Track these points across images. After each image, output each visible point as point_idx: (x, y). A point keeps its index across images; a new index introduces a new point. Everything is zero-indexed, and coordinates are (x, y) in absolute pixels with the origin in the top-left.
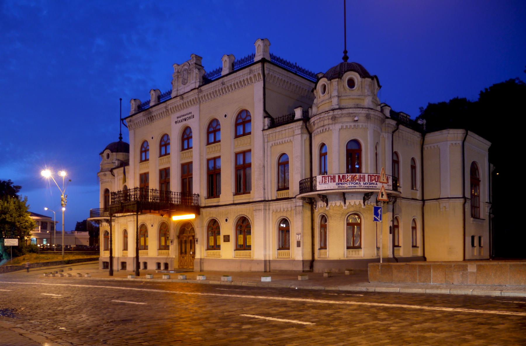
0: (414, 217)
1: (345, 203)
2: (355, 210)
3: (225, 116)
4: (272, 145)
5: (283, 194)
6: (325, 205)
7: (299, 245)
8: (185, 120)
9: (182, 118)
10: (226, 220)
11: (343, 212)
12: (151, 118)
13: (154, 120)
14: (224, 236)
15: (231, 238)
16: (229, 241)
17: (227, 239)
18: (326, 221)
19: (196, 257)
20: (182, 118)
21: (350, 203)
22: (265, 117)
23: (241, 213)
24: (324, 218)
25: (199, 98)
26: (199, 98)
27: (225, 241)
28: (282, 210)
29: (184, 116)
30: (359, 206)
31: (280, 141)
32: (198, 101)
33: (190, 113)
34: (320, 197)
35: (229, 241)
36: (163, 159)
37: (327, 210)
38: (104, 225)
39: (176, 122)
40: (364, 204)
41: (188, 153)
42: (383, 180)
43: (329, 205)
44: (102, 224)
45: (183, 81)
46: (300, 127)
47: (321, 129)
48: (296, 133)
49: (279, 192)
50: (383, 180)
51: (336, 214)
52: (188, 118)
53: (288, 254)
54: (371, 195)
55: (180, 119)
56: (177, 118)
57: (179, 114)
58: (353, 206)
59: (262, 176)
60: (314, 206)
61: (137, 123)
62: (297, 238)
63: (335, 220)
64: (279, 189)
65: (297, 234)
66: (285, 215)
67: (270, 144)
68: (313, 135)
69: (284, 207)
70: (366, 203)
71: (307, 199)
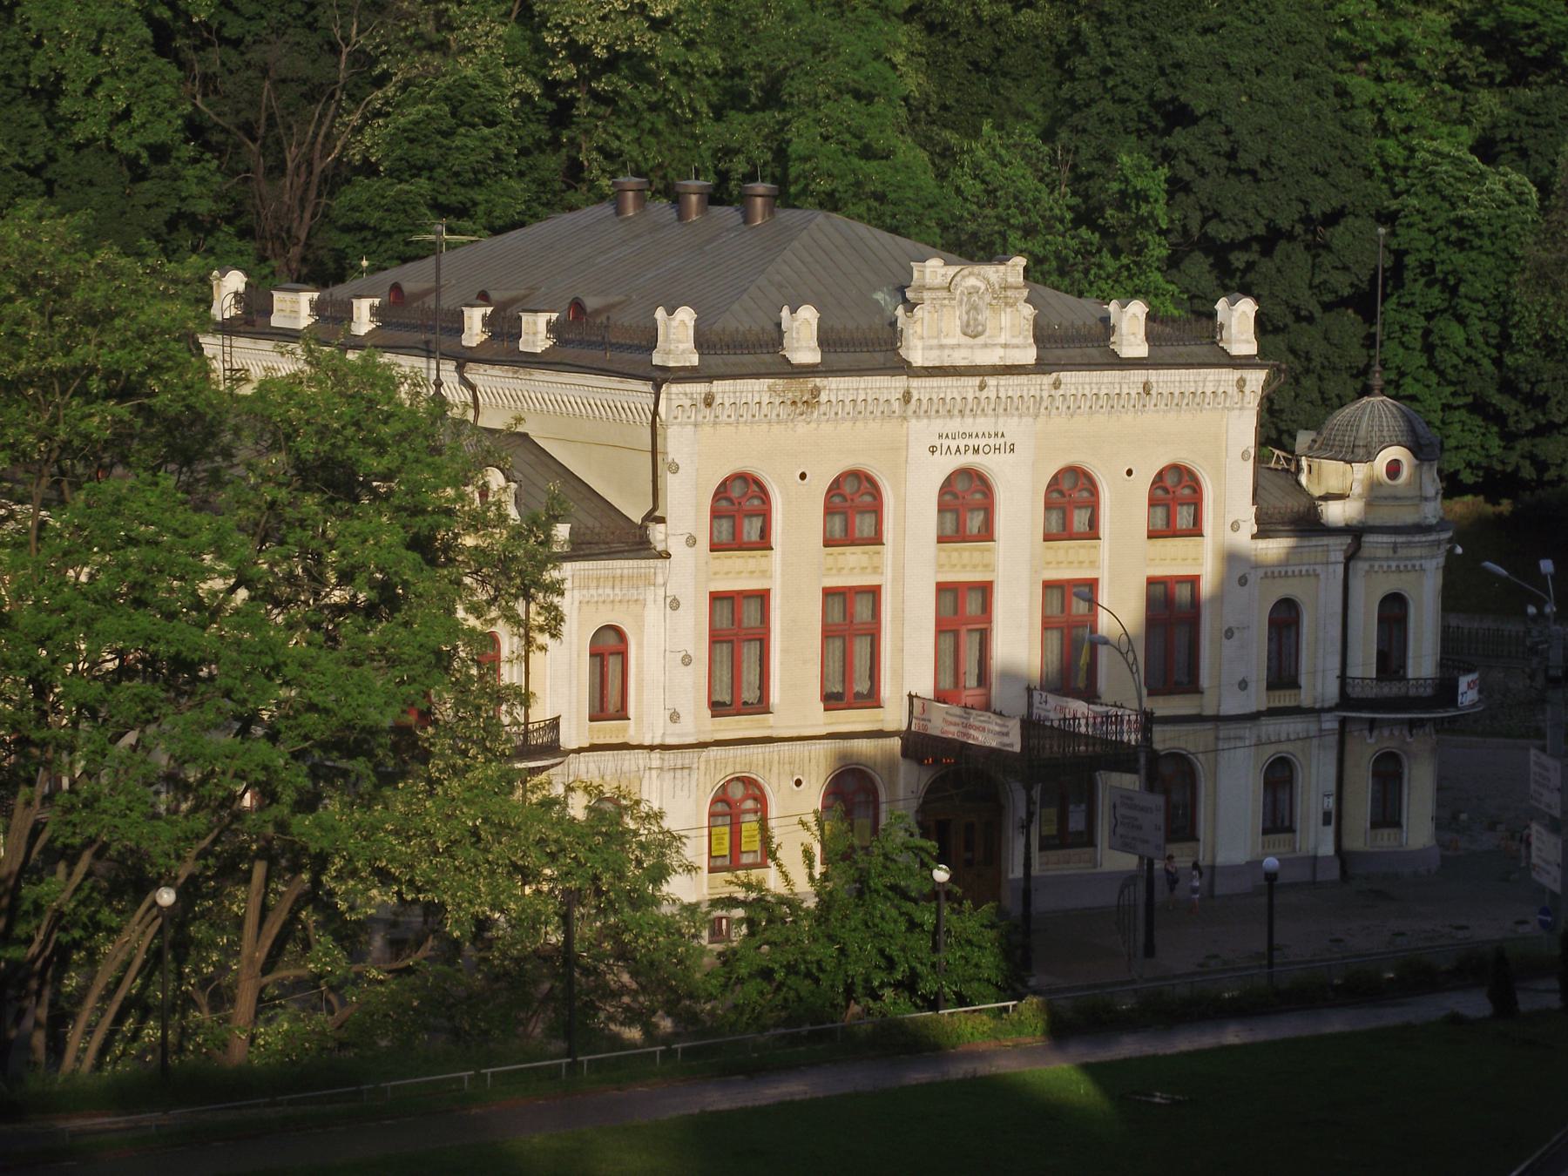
5: (1285, 699)
8: (976, 451)
9: (962, 443)
20: (962, 443)
29: (971, 436)
32: (1038, 407)
33: (996, 435)
39: (933, 450)
48: (1332, 559)
49: (1271, 693)
52: (987, 450)
56: (940, 436)
57: (955, 425)
64: (1271, 686)
66: (1285, 749)
68: (1360, 567)
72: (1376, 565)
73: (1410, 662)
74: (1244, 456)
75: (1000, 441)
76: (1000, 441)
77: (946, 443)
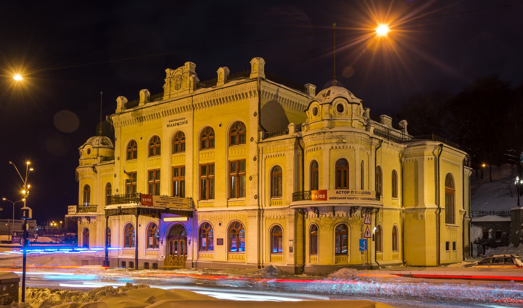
0: (394, 225)
1: (334, 215)
2: (343, 221)
3: (220, 125)
4: (266, 157)
6: (317, 215)
7: (291, 251)
8: (178, 125)
9: (174, 122)
10: (220, 224)
11: (332, 223)
12: (140, 118)
13: (143, 120)
14: (218, 239)
15: (224, 241)
16: (222, 244)
17: (220, 242)
18: (316, 230)
19: (187, 259)
20: (174, 122)
21: (338, 215)
22: (259, 131)
23: (238, 219)
24: (314, 228)
25: (193, 105)
26: (193, 105)
27: (218, 244)
28: (275, 217)
29: (177, 120)
30: (346, 218)
31: (275, 154)
33: (183, 119)
34: (312, 209)
35: (222, 244)
36: (153, 160)
37: (318, 221)
38: (84, 222)
39: (168, 126)
40: (351, 216)
41: (180, 156)
42: (368, 222)
43: (320, 216)
44: (81, 221)
45: (175, 87)
46: (293, 144)
47: (313, 147)
50: (368, 222)
51: (326, 224)
52: (181, 123)
53: (281, 258)
54: (357, 209)
55: (172, 123)
56: (170, 122)
58: (341, 218)
59: (256, 185)
60: (306, 216)
61: (124, 122)
62: (290, 244)
63: (325, 230)
65: (289, 240)
66: (278, 222)
67: (264, 156)
69: (278, 215)
70: (352, 215)
71: (299, 209)
72: (307, 149)
73: (319, 188)
74: (255, 115)
75: (183, 120)
76: (183, 120)
77: (171, 123)
